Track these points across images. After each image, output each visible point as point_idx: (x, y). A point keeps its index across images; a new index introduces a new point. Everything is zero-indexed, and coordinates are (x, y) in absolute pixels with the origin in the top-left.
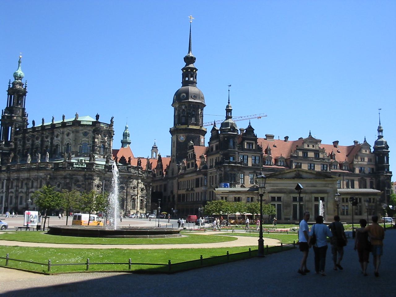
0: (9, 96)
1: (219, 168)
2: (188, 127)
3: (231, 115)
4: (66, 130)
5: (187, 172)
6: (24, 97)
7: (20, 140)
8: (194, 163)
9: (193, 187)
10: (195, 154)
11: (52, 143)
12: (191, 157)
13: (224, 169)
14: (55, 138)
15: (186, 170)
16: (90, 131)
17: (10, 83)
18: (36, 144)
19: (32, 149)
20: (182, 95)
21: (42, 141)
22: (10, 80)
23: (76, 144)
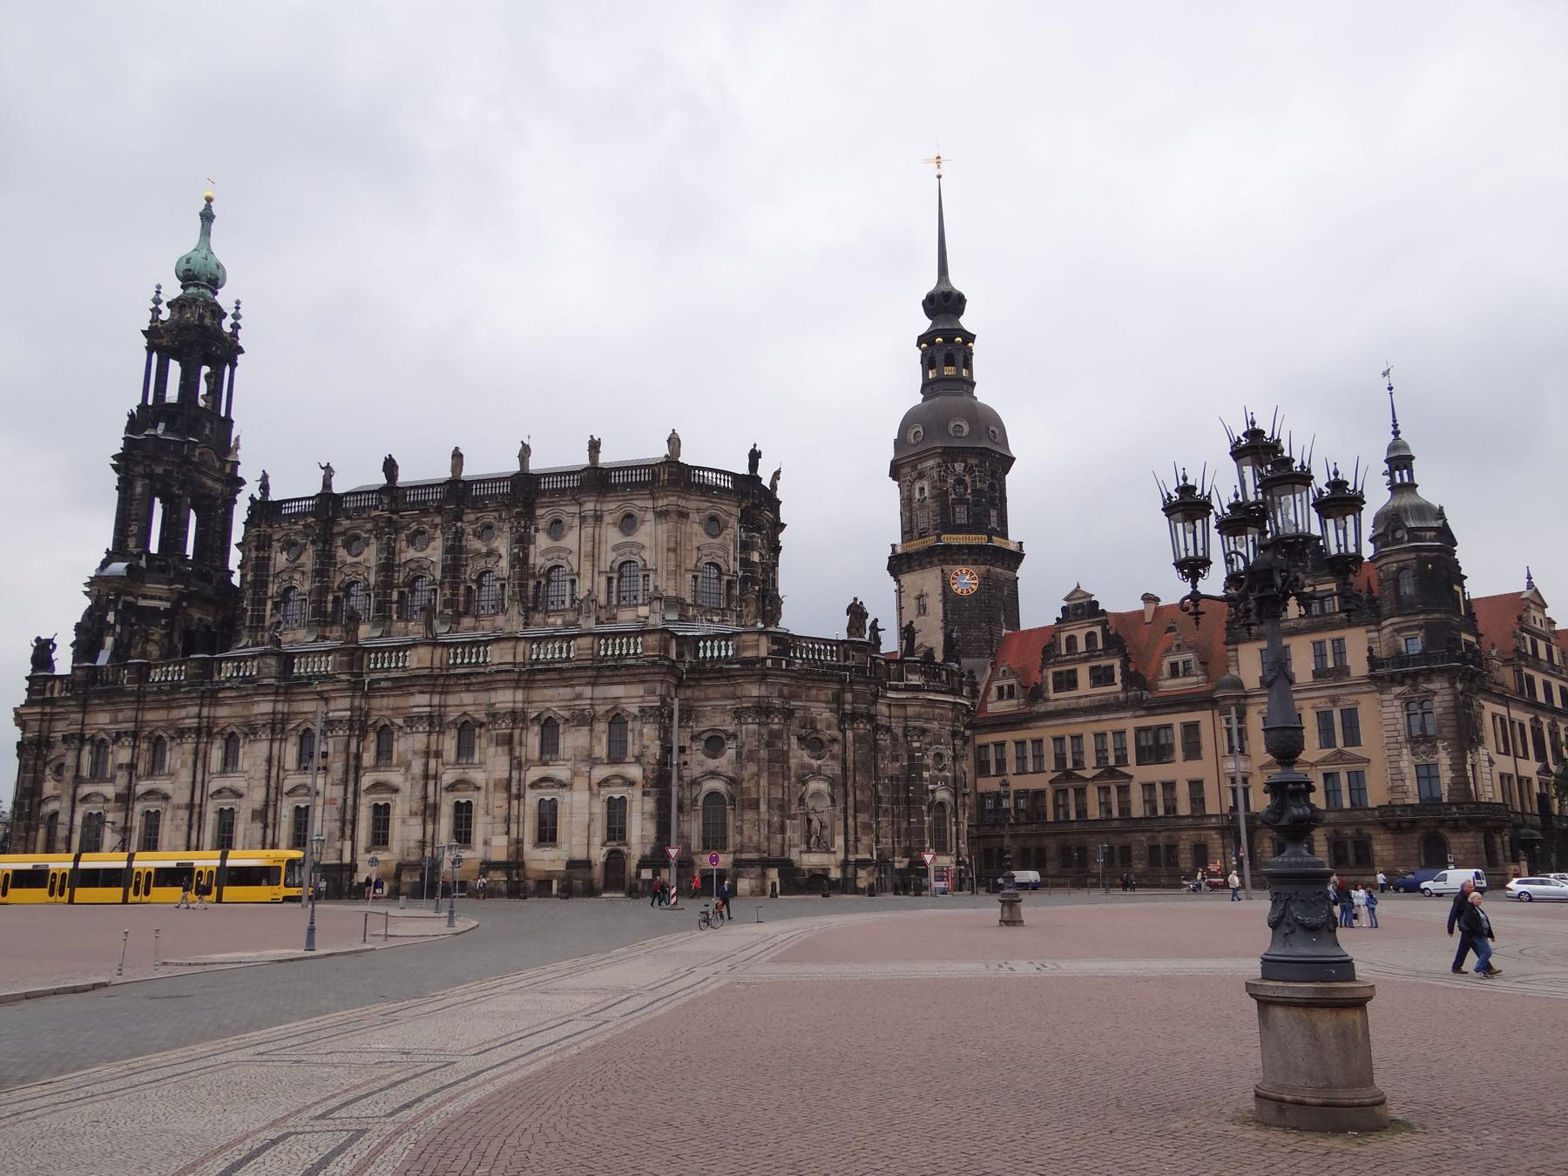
0: (155, 356)
1: (1394, 680)
2: (990, 540)
3: (1411, 476)
4: (612, 507)
5: (1041, 708)
6: (227, 369)
7: (289, 545)
8: (1117, 671)
9: (1112, 762)
10: (1116, 634)
11: (520, 560)
12: (1081, 646)
13: (1453, 686)
14: (542, 541)
15: (1047, 700)
16: (731, 515)
17: (157, 301)
18: (413, 565)
19: (386, 585)
20: (952, 425)
21: (455, 552)
22: (159, 287)
23: (678, 566)
